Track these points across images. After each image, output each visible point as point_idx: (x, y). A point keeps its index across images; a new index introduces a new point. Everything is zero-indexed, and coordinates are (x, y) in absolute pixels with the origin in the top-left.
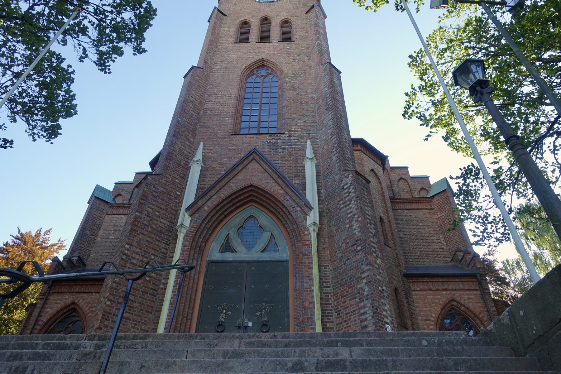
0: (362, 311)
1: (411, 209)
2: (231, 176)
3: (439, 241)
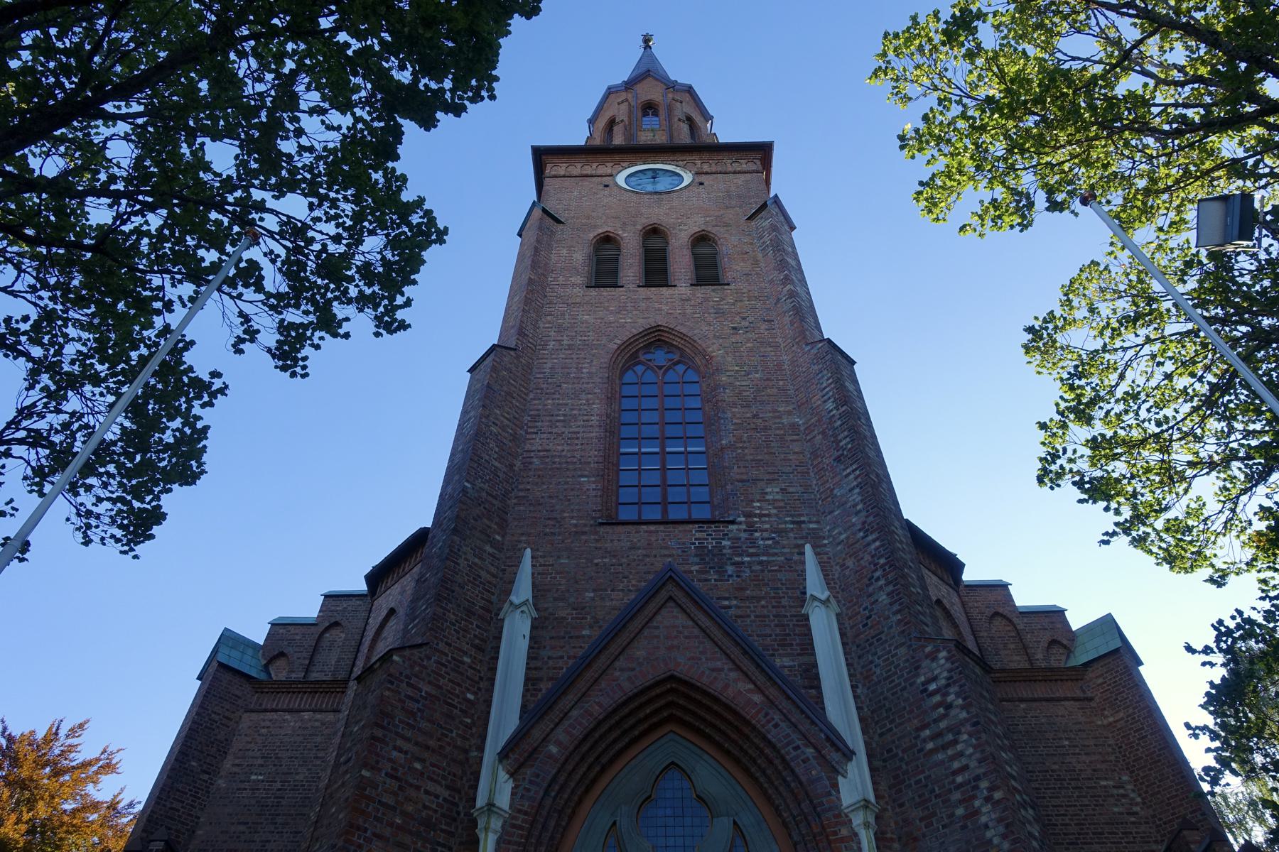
1: (1034, 700)
3: (1121, 791)
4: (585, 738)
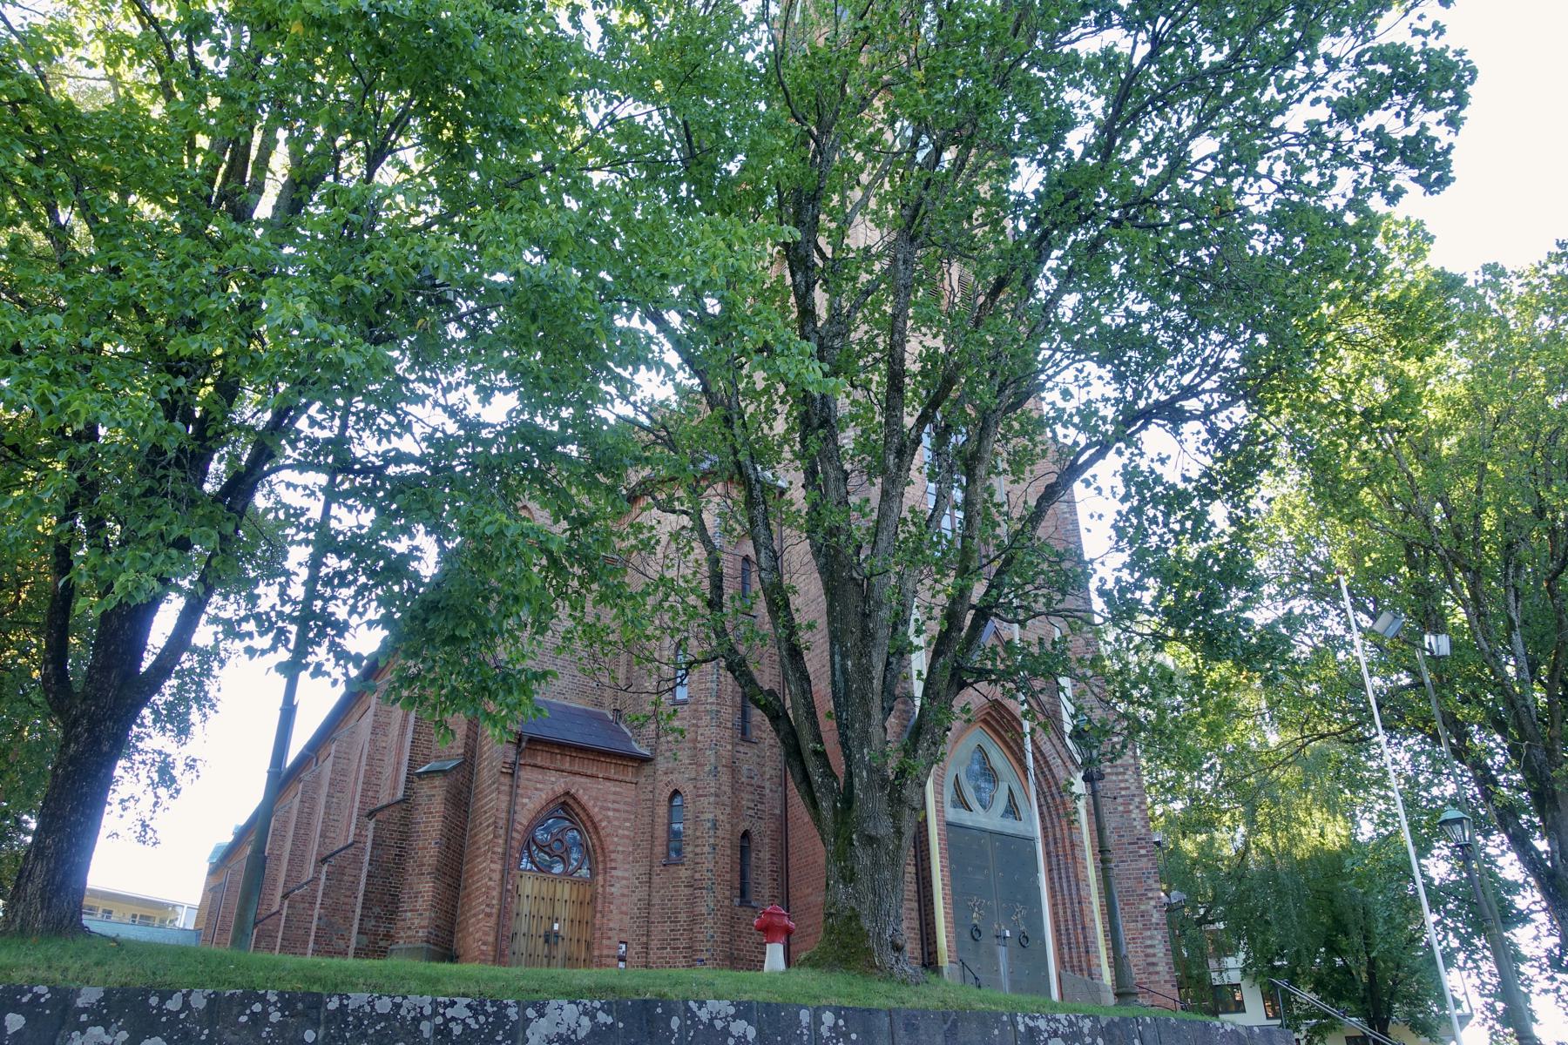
0: (1149, 942)
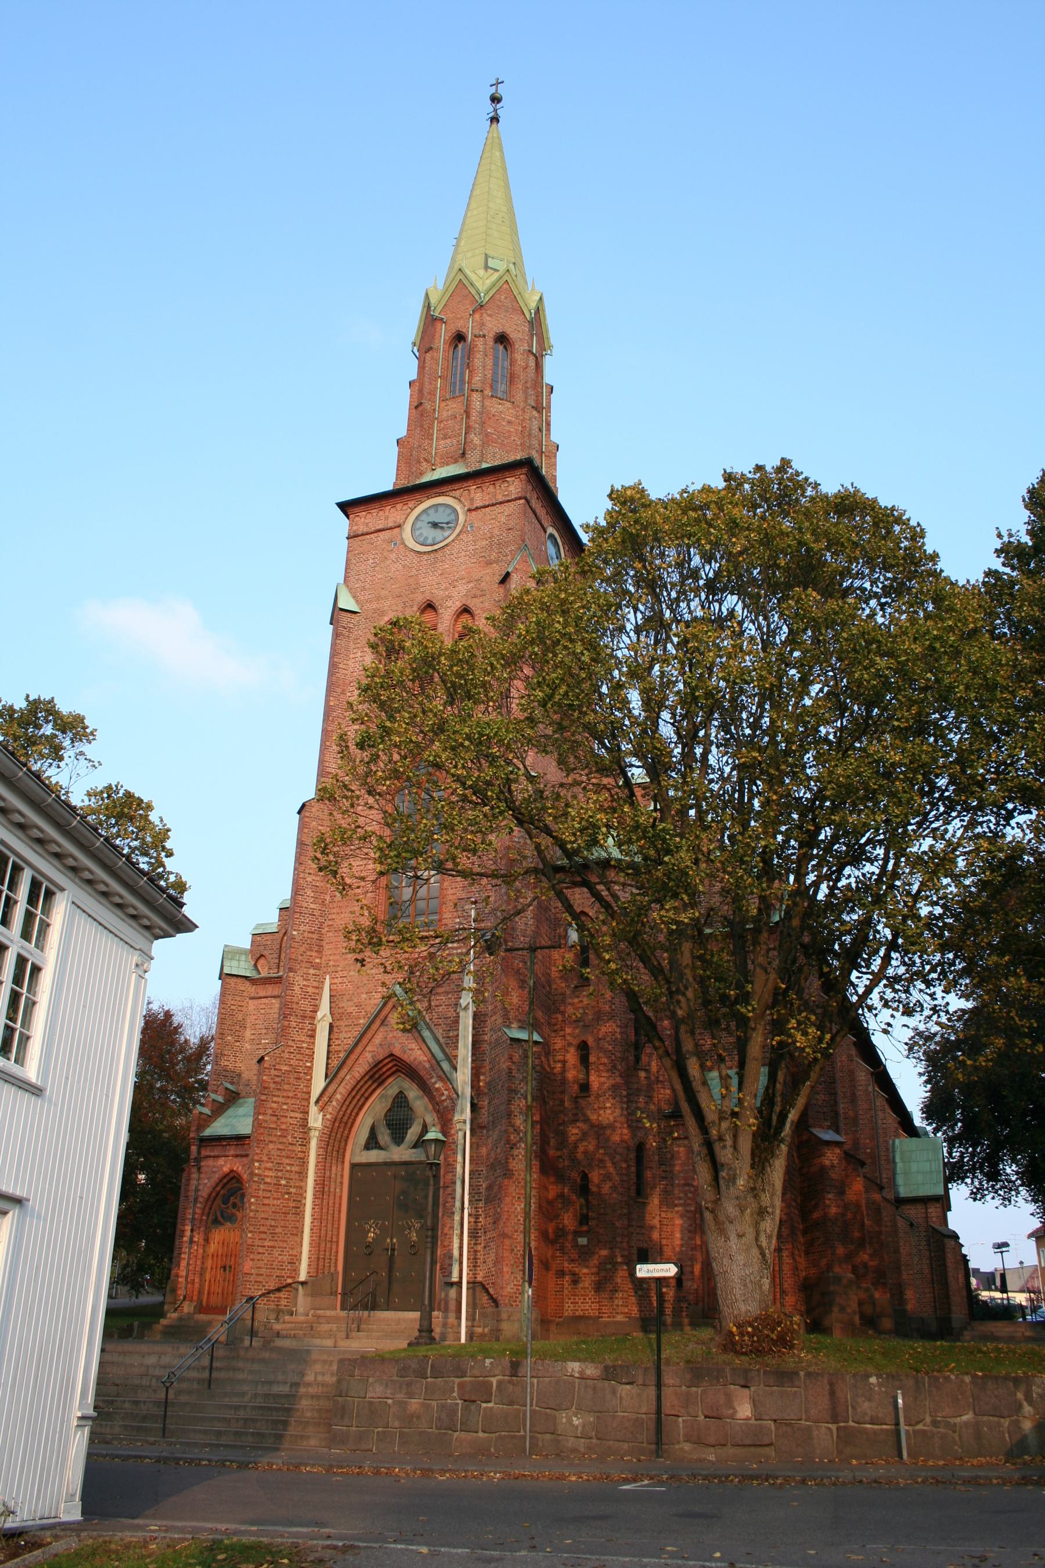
2: (364, 1041)
4: (353, 1089)
